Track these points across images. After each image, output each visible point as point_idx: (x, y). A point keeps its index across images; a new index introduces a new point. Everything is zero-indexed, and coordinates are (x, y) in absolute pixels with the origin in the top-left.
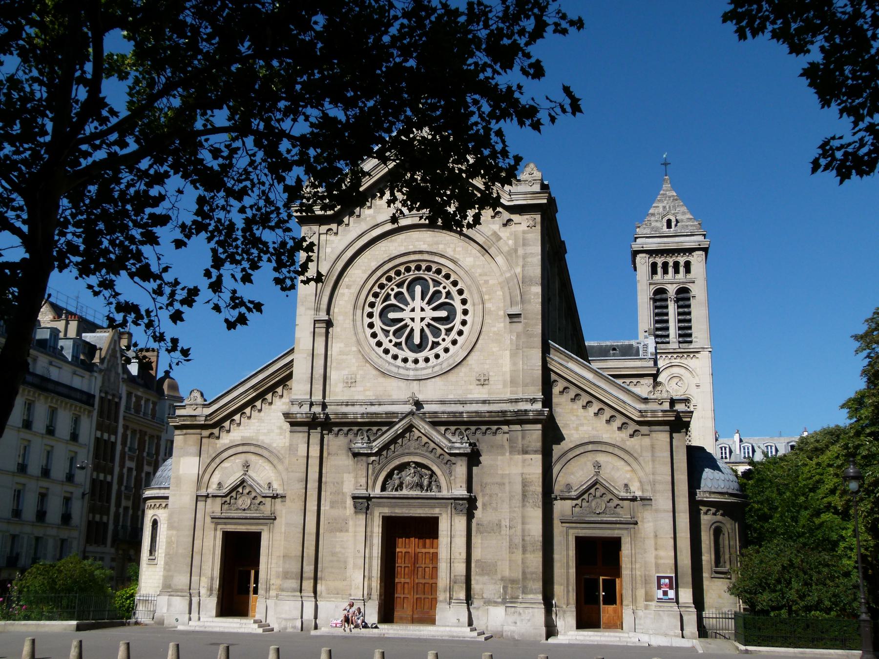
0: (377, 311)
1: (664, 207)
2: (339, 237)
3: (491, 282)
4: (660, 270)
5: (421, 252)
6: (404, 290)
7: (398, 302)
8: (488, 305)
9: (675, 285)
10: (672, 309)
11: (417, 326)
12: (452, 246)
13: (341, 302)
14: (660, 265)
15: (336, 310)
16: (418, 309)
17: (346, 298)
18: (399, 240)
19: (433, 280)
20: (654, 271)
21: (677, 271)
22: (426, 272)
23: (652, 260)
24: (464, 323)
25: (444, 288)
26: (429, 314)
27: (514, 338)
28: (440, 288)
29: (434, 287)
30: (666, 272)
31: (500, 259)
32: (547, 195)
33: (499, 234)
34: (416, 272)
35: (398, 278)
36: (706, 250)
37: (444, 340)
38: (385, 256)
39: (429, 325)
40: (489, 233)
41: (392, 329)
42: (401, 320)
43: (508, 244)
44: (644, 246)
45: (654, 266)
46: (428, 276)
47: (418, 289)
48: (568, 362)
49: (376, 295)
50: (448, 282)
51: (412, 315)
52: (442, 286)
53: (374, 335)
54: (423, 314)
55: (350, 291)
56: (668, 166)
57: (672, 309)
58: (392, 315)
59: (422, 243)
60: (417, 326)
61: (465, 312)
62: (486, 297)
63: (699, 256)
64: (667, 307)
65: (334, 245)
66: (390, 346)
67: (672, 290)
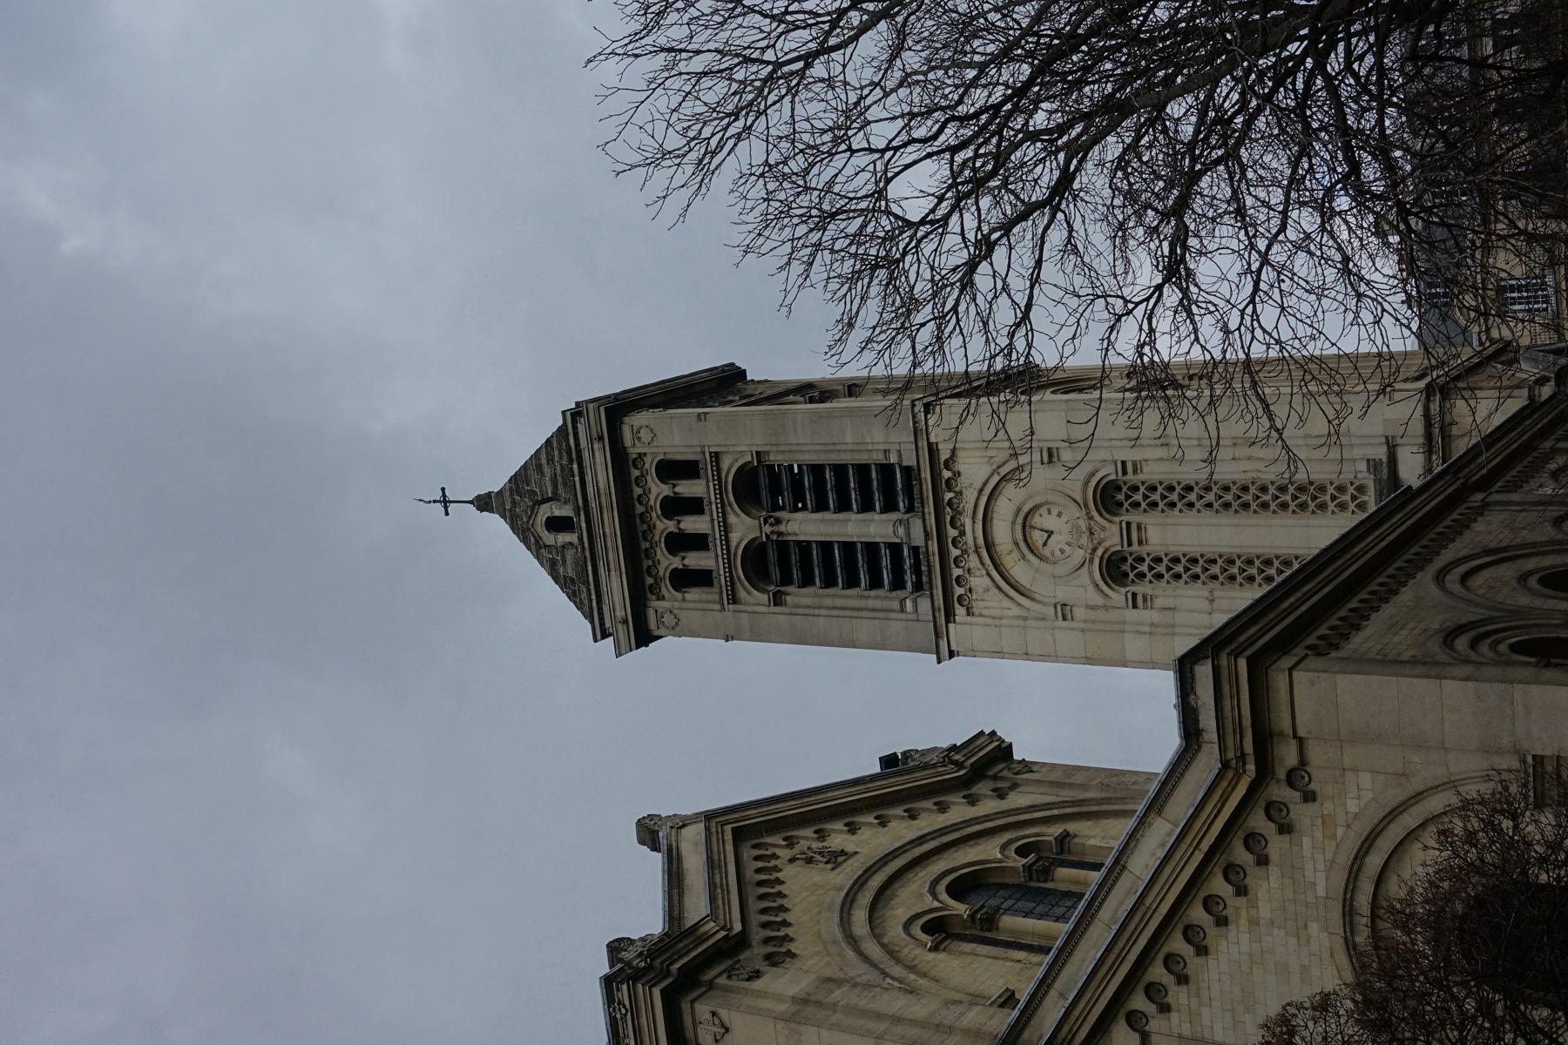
4: (695, 560)
9: (732, 519)
10: (805, 526)
14: (676, 563)
20: (703, 578)
21: (694, 506)
23: (667, 589)
30: (699, 542)
44: (620, 613)
45: (686, 579)
57: (805, 526)
63: (636, 433)
64: (804, 547)
67: (744, 527)
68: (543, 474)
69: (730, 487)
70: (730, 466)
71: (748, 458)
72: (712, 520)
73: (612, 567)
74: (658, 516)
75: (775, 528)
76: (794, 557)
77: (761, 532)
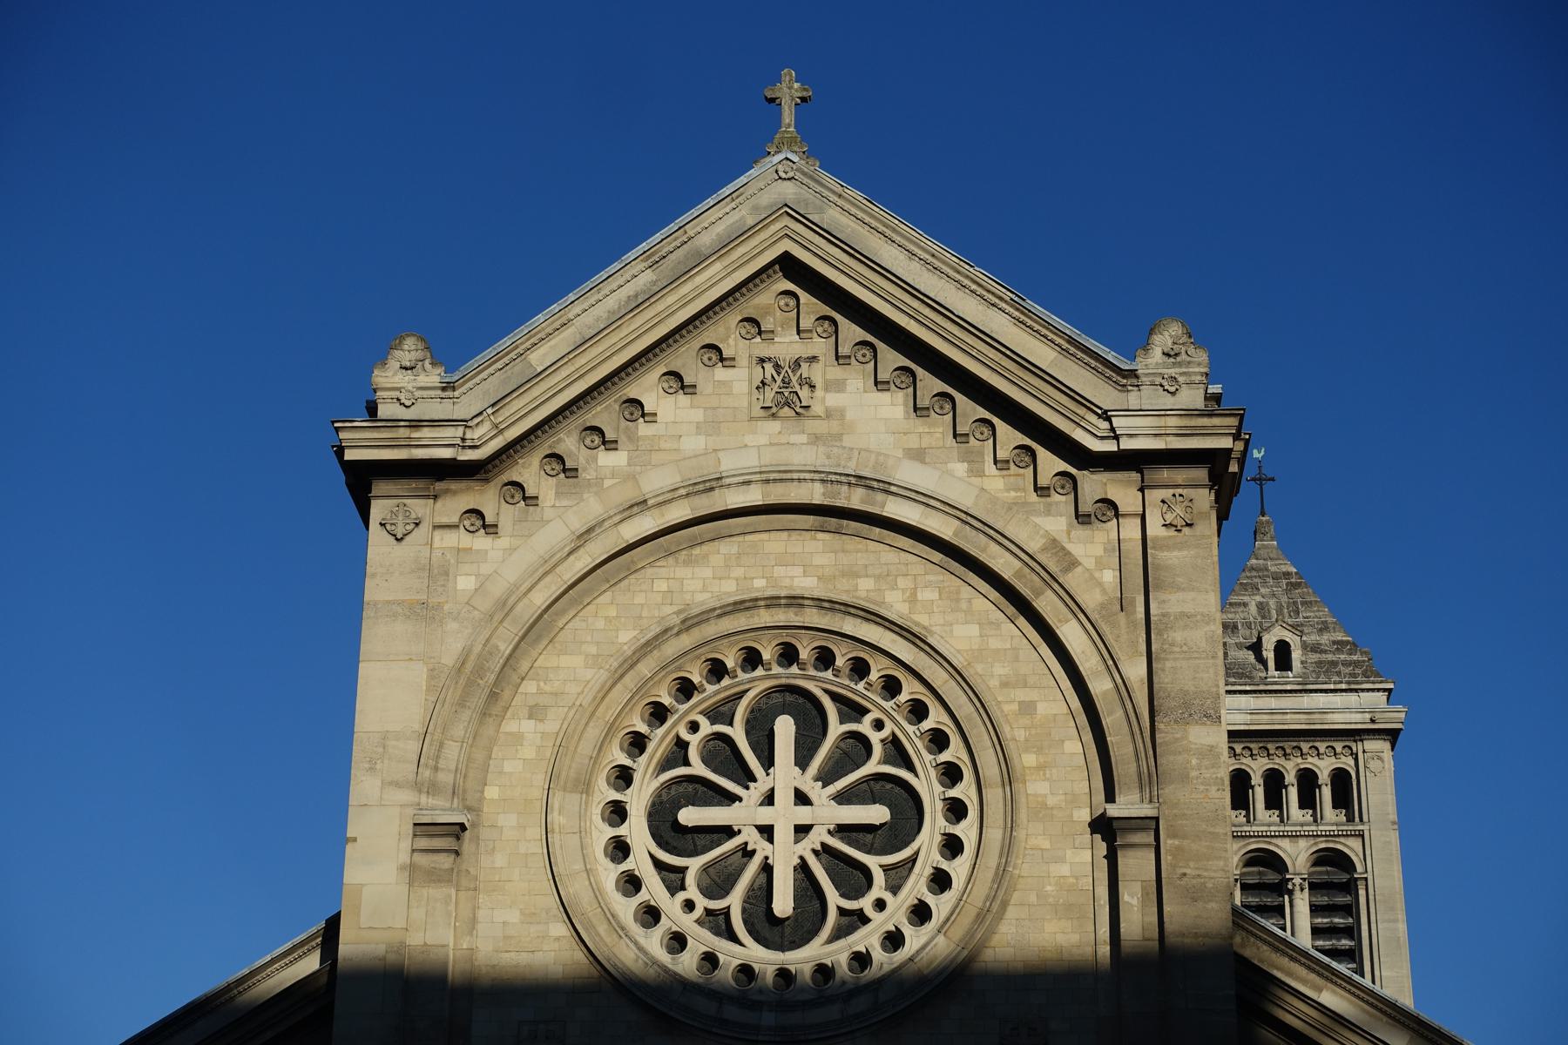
0: (638, 799)
1: (1261, 607)
2: (503, 542)
3: (1042, 709)
5: (795, 601)
6: (738, 733)
7: (715, 771)
8: (1035, 788)
9: (1302, 843)
11: (784, 855)
12: (902, 582)
13: (508, 767)
14: (1257, 780)
15: (491, 792)
16: (784, 797)
17: (528, 752)
18: (716, 560)
19: (835, 697)
22: (812, 672)
24: (952, 846)
25: (879, 725)
26: (827, 812)
27: (1134, 902)
28: (865, 727)
29: (841, 723)
30: (1274, 800)
31: (1072, 635)
32: (1234, 421)
33: (1069, 547)
34: (776, 670)
35: (711, 688)
36: (1392, 735)
37: (880, 905)
38: (668, 610)
39: (825, 851)
40: (1032, 547)
41: (694, 864)
42: (728, 832)
43: (1100, 584)
46: (816, 683)
47: (785, 729)
48: (1319, 990)
49: (637, 743)
50: (888, 705)
51: (765, 815)
52: (868, 719)
53: (632, 883)
54: (803, 815)
55: (541, 727)
56: (1267, 486)
58: (689, 816)
59: (798, 571)
60: (784, 855)
61: (956, 810)
62: (1029, 760)
65: (486, 569)
66: (687, 923)
67: (1298, 856)
68: (1321, 631)
69: (1331, 845)
70: (1351, 847)
71: (1359, 868)
72: (1302, 825)
73: (1254, 717)
74: (1298, 765)
75: (1298, 888)
76: (1269, 900)
77: (1295, 874)
